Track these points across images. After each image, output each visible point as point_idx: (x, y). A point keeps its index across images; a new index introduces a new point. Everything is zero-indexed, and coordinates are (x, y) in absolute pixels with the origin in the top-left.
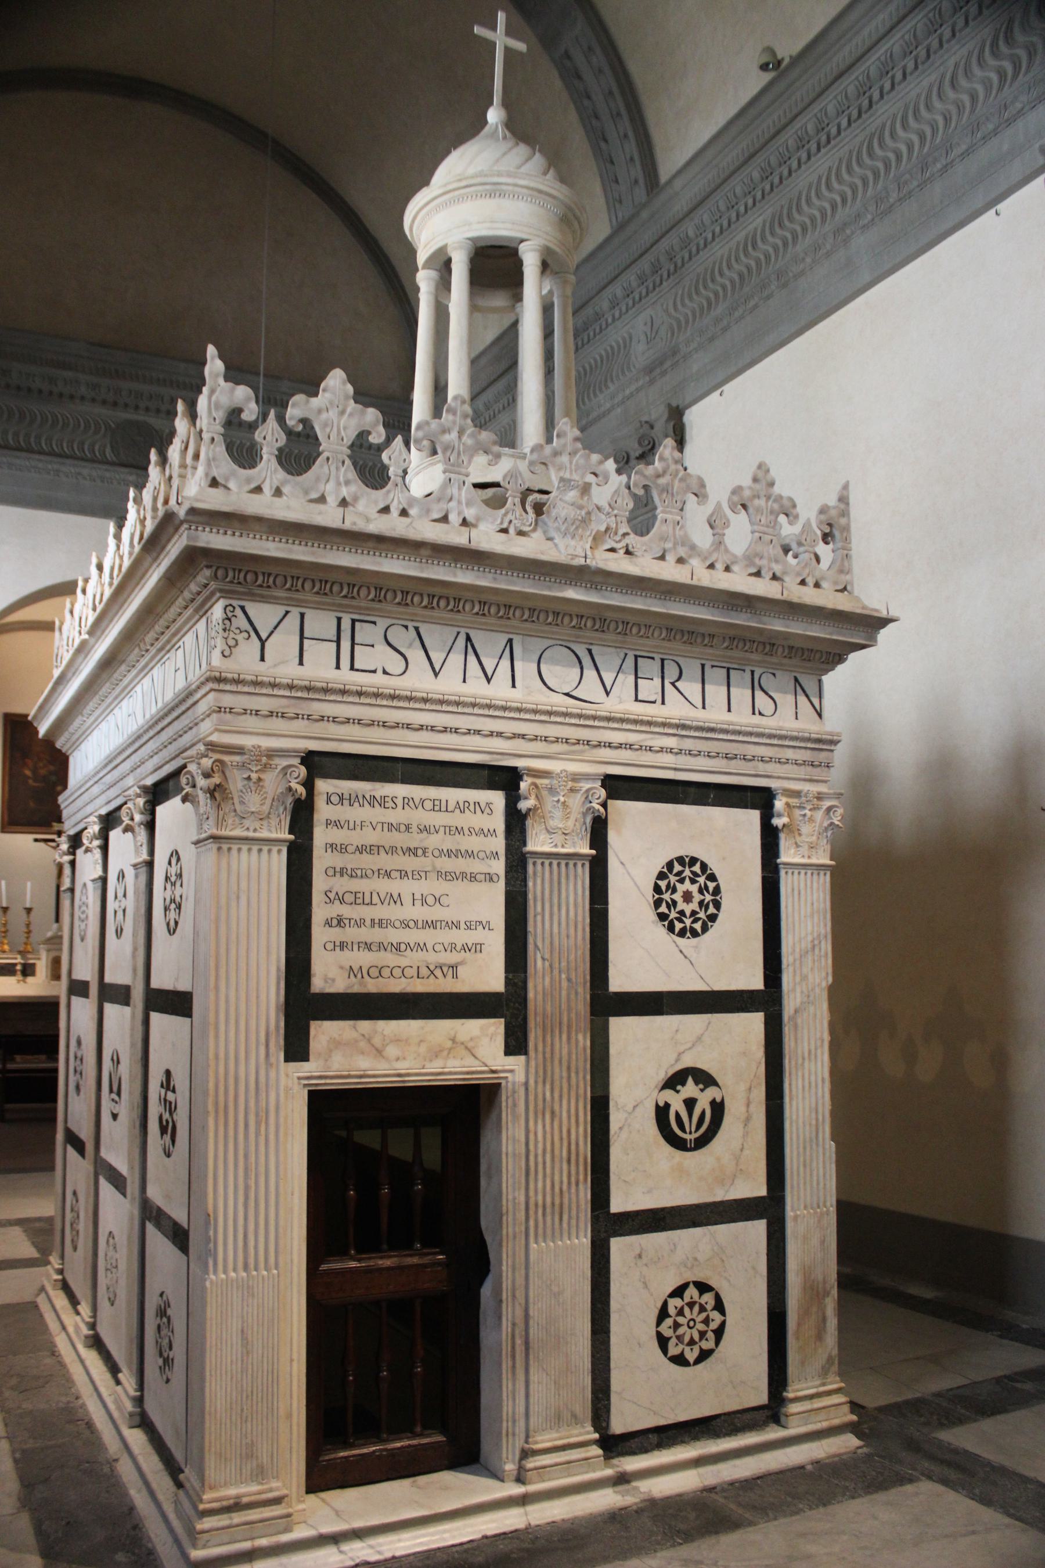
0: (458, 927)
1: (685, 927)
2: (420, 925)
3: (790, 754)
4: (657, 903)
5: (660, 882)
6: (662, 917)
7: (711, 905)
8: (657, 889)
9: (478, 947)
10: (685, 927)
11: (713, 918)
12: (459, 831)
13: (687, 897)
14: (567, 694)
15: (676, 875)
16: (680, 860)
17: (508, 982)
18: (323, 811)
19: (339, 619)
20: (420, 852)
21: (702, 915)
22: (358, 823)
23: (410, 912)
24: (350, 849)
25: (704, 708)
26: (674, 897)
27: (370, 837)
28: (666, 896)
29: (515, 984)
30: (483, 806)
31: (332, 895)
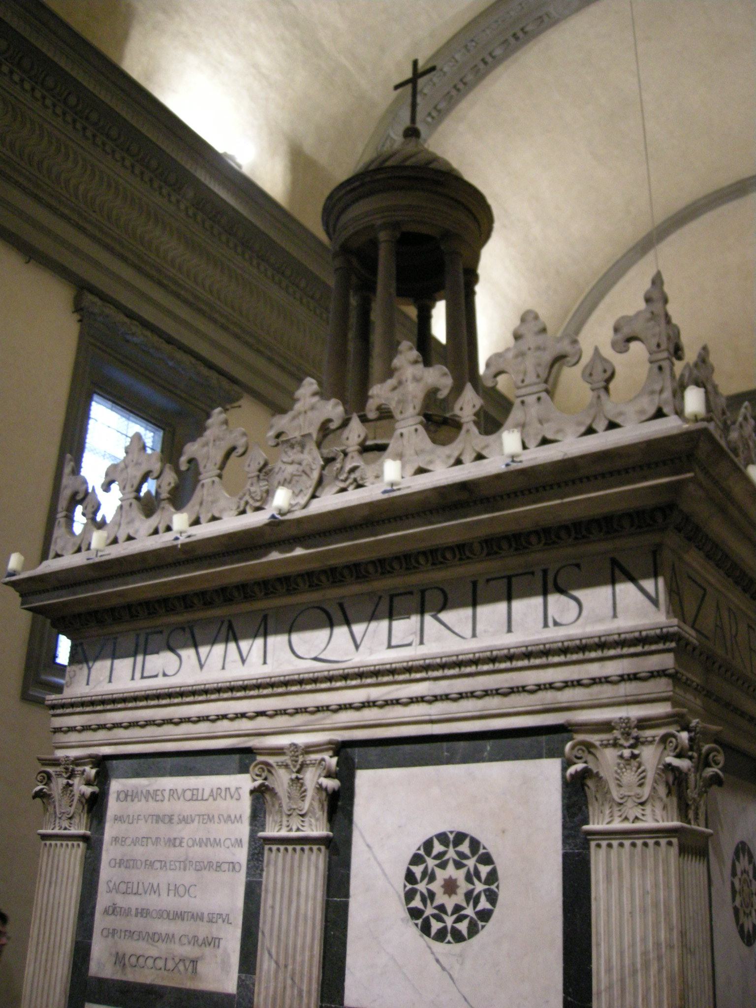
0: (202, 919)
1: (445, 928)
2: (171, 917)
3: (594, 670)
4: (409, 896)
5: (414, 869)
6: (415, 913)
7: (483, 898)
8: (410, 877)
9: (217, 941)
10: (445, 928)
11: (485, 916)
12: (210, 818)
13: (450, 887)
14: (316, 659)
15: (436, 858)
16: (442, 838)
17: (241, 984)
18: (113, 806)
19: (138, 636)
20: (178, 842)
21: (469, 911)
22: (136, 817)
23: (168, 902)
24: (129, 841)
25: (474, 635)
26: (432, 887)
27: (143, 829)
28: (422, 887)
29: (247, 987)
30: (233, 790)
31: (111, 885)
